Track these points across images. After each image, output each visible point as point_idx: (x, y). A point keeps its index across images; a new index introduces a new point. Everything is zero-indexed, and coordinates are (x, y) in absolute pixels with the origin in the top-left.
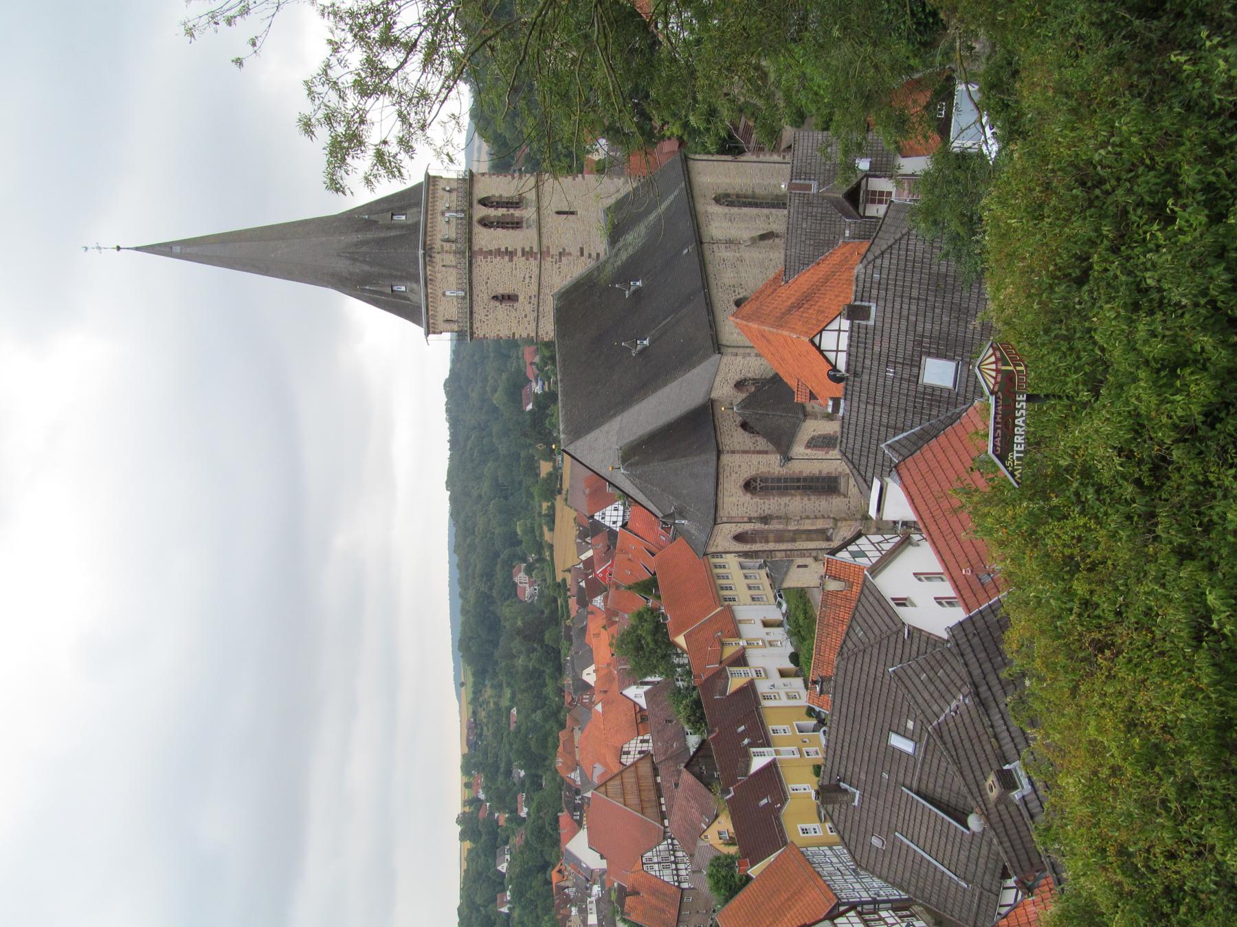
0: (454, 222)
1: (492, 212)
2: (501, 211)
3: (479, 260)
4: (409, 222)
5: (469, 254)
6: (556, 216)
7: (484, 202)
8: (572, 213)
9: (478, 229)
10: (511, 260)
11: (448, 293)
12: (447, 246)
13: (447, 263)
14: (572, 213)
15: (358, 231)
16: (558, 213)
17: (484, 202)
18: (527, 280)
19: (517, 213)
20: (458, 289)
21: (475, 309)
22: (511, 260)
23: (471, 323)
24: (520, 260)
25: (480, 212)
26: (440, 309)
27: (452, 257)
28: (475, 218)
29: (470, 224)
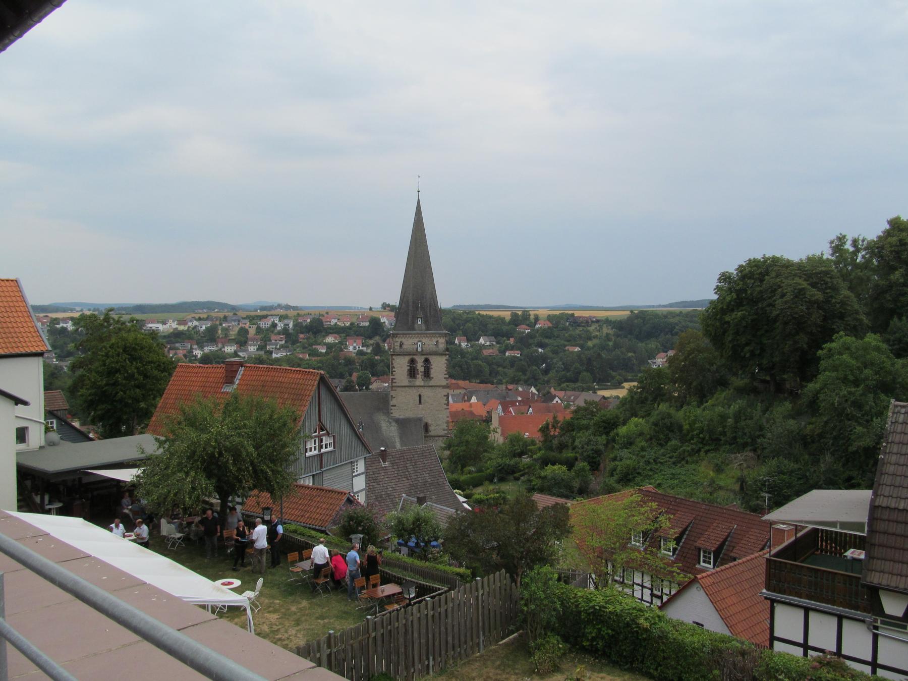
4: (416, 326)
7: (427, 361)
8: (420, 402)
9: (408, 358)
14: (420, 402)
15: (413, 302)
16: (420, 396)
17: (427, 361)
25: (420, 361)
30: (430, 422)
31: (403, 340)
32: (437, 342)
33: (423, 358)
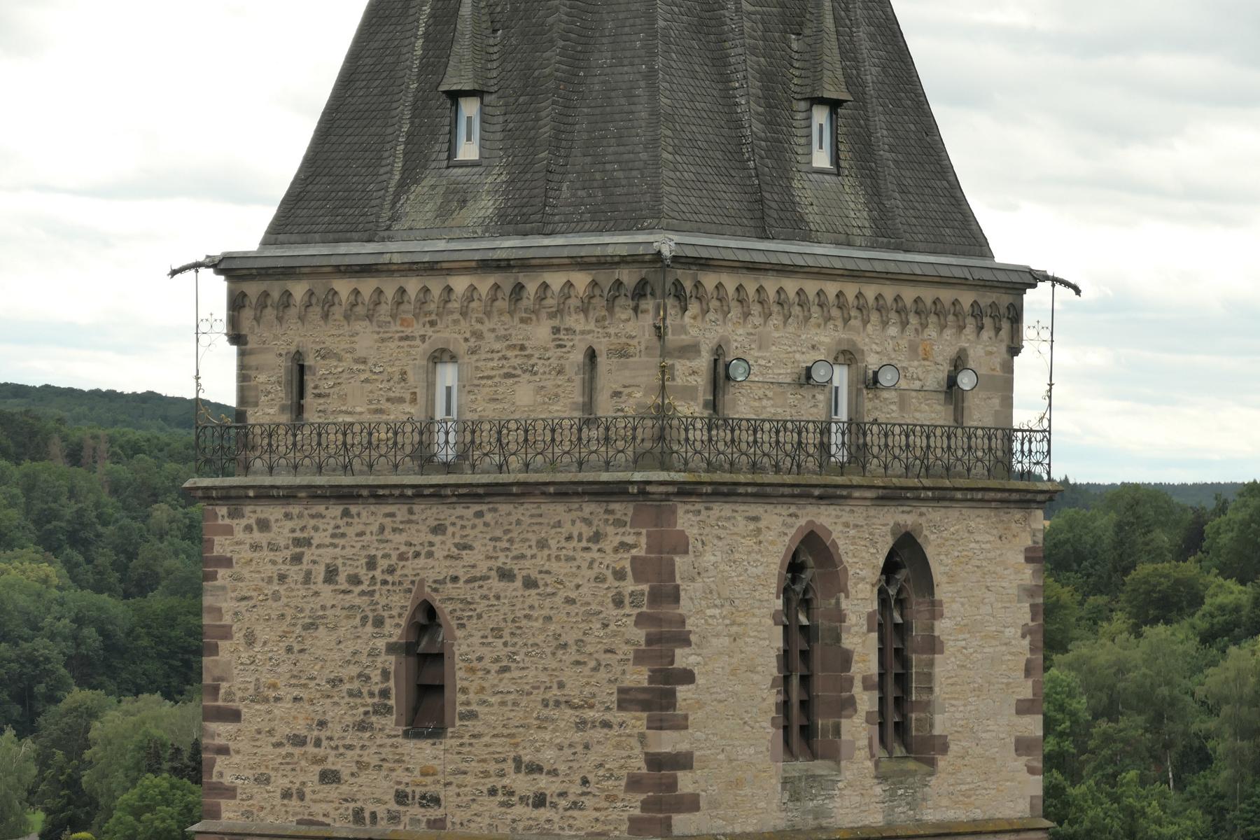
0: (810, 408)
1: (859, 602)
2: (863, 649)
3: (624, 537)
4: (805, 192)
5: (649, 482)
7: (905, 563)
9: (778, 529)
10: (627, 699)
11: (448, 375)
12: (693, 373)
13: (609, 375)
17: (905, 563)
18: (522, 784)
19: (857, 729)
20: (469, 429)
21: (369, 517)
22: (627, 699)
23: (288, 495)
24: (625, 745)
25: (860, 540)
26: (365, 338)
27: (640, 397)
28: (827, 518)
29: (802, 493)
32: (959, 363)
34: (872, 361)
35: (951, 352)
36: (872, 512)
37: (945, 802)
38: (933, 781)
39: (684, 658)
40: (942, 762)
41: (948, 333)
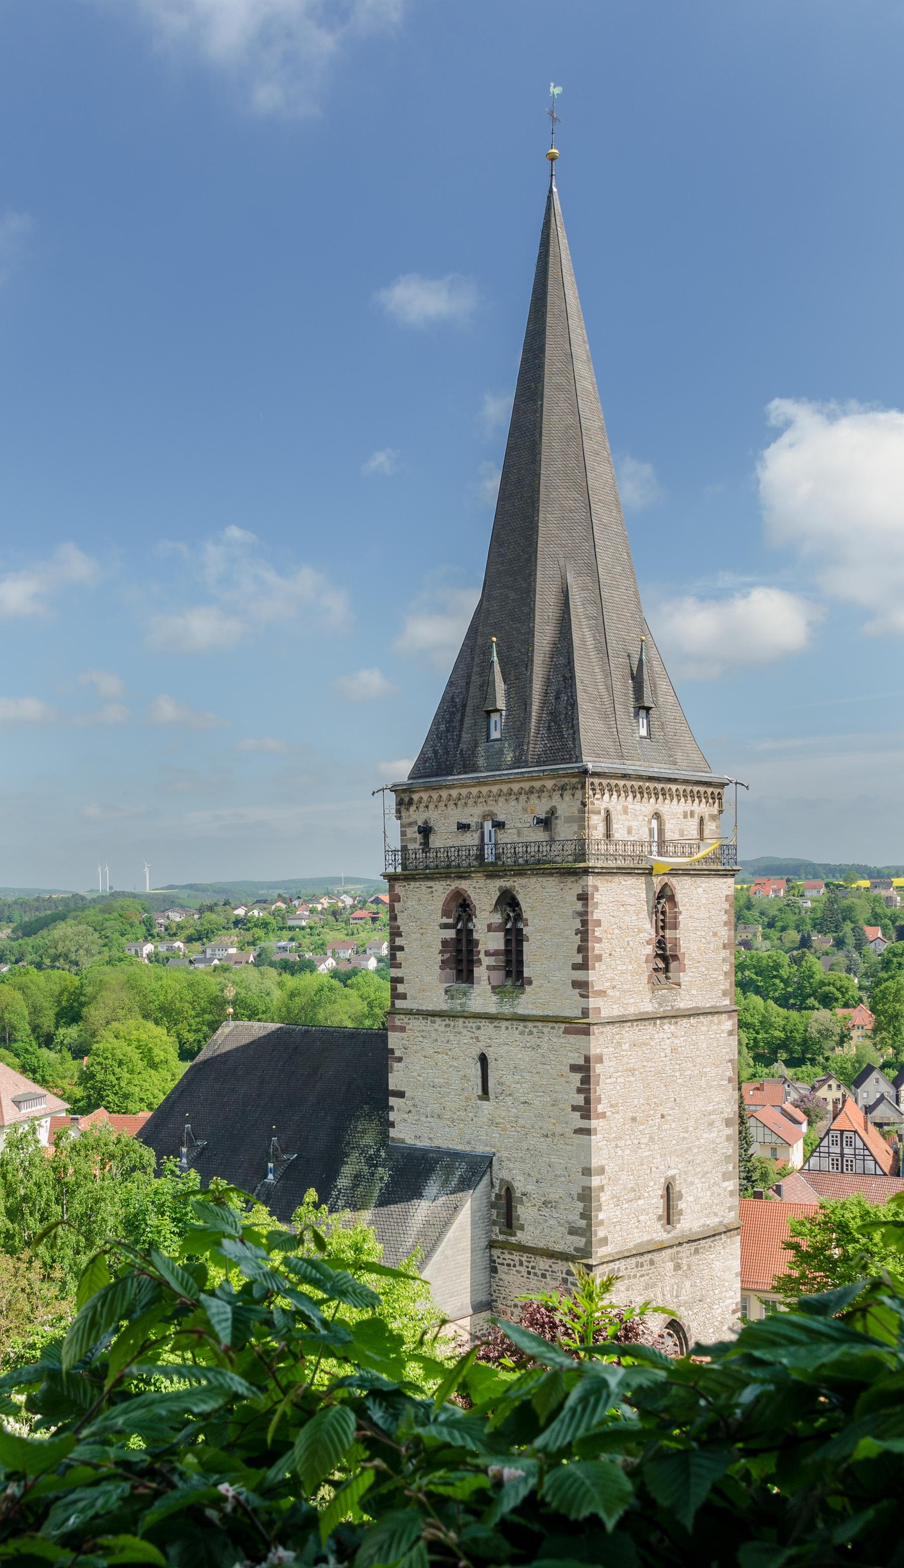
2: (489, 941)
6: (475, 1052)
7: (508, 901)
8: (485, 1092)
14: (485, 1092)
16: (483, 1059)
17: (508, 901)
25: (483, 894)
28: (464, 885)
30: (519, 1187)
31: (433, 816)
33: (494, 887)
34: (501, 818)
35: (547, 808)
36: (488, 881)
37: (530, 1006)
38: (523, 996)
39: (399, 941)
40: (528, 988)
41: (544, 800)
